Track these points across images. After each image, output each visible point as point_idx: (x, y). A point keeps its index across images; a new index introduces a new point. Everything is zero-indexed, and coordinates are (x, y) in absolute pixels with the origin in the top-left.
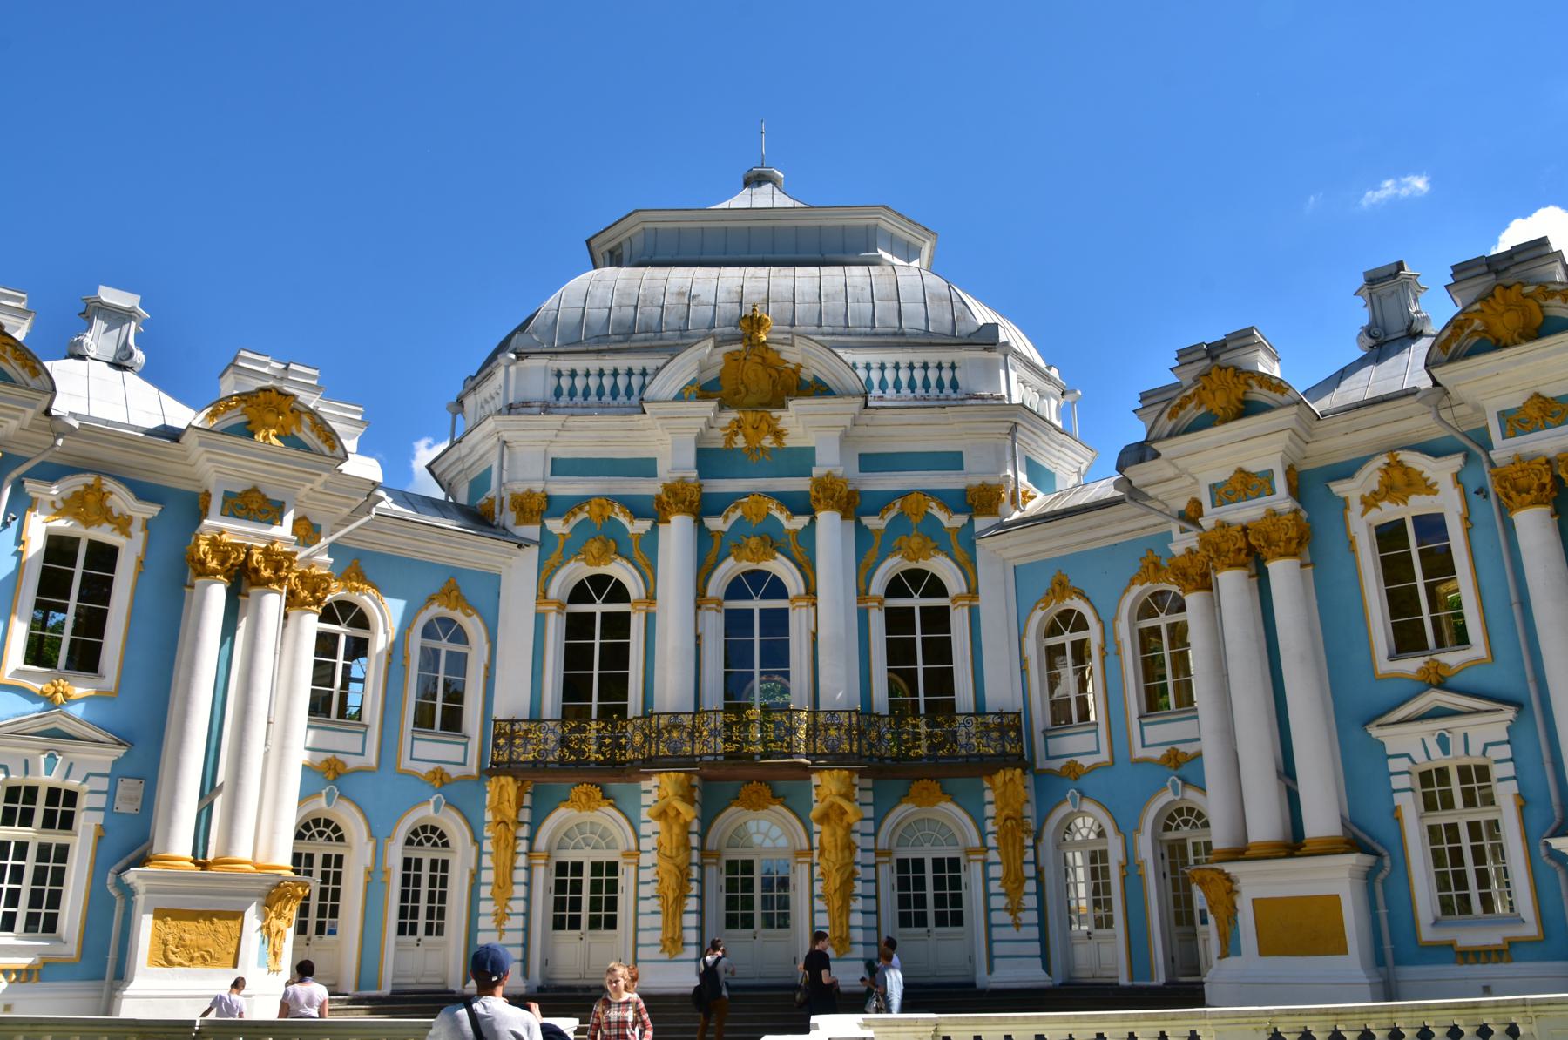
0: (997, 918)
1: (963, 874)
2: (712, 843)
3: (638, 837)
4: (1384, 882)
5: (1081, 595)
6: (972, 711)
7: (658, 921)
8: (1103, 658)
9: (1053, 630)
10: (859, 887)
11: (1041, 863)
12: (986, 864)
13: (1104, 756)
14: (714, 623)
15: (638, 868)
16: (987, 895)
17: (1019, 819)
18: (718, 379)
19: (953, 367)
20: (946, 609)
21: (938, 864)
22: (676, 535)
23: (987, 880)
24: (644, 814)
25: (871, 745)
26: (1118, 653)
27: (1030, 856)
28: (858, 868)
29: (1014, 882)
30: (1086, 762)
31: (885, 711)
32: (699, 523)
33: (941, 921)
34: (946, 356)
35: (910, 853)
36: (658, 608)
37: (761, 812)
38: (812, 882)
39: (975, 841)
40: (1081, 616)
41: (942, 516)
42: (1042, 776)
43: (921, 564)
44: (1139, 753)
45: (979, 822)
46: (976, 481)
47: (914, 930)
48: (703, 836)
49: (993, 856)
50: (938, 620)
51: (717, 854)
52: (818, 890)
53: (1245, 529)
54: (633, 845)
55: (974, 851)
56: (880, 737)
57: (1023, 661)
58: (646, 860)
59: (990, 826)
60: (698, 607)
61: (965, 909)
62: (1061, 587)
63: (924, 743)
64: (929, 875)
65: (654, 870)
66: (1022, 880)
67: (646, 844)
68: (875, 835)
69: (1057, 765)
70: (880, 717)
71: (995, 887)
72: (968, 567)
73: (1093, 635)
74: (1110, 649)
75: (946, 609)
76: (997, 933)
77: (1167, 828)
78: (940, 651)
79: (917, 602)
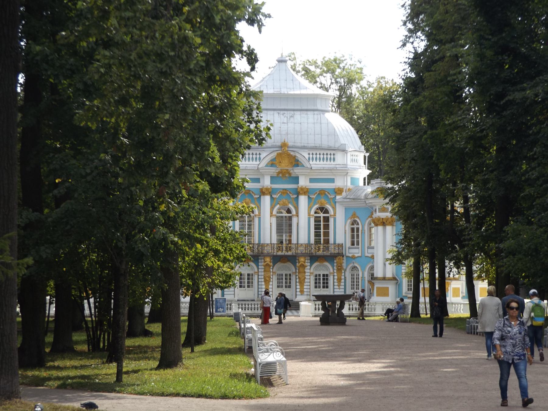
0: (335, 287)
1: (329, 277)
2: (274, 270)
3: (258, 269)
4: (399, 285)
5: (358, 218)
6: (333, 243)
7: (264, 287)
8: (362, 233)
9: (353, 224)
10: (306, 280)
11: (346, 276)
12: (334, 276)
13: (360, 255)
14: (274, 220)
15: (258, 275)
16: (334, 282)
17: (341, 266)
18: (275, 158)
19: (334, 154)
20: (328, 218)
21: (324, 275)
22: (266, 200)
23: (334, 279)
24: (260, 264)
25: (310, 251)
26: (364, 233)
27: (343, 274)
28: (306, 277)
29: (339, 280)
30: (356, 255)
31: (313, 243)
32: (271, 196)
33: (324, 287)
34: (332, 152)
35: (318, 273)
36: (261, 217)
37: (285, 264)
38: (296, 279)
39: (332, 271)
40: (358, 223)
41: (329, 196)
42: (347, 257)
43: (323, 206)
44: (367, 255)
45: (333, 267)
46: (337, 187)
47: (318, 289)
48: (273, 269)
49: (335, 274)
50: (327, 219)
51: (275, 273)
52: (298, 281)
53: (383, 219)
54: (256, 270)
55: (332, 273)
56: (312, 249)
57: (345, 231)
58: (260, 274)
59: (335, 268)
60: (271, 216)
61: (329, 285)
62: (354, 215)
63: (322, 250)
64: (322, 277)
65: (263, 276)
66: (341, 279)
67: (260, 270)
68: (310, 269)
69: (350, 255)
70: (312, 244)
71: (335, 281)
72: (334, 208)
73: (360, 227)
74: (363, 232)
75: (328, 217)
76: (335, 290)
77: (371, 270)
78: (327, 227)
79: (322, 215)
